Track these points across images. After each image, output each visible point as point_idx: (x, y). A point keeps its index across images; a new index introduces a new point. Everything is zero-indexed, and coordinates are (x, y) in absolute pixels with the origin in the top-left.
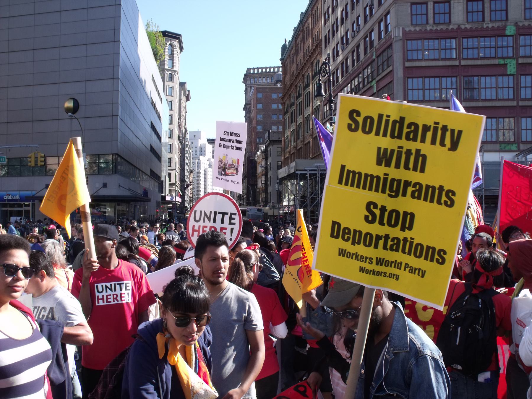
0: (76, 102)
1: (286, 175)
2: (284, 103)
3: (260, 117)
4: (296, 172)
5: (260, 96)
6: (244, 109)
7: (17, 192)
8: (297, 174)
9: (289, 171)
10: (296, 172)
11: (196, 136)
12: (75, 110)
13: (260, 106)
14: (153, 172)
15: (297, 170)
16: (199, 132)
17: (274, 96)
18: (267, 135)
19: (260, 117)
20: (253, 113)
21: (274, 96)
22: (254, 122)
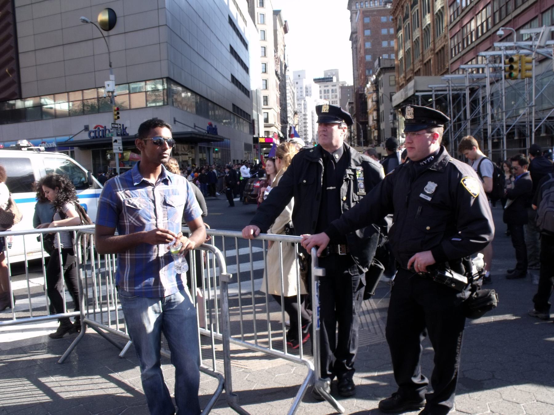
0: (111, 12)
1: (402, 100)
2: (396, 18)
3: (368, 45)
4: (417, 94)
5: (367, 20)
6: (351, 39)
7: (54, 139)
8: (418, 96)
9: (407, 94)
10: (417, 94)
11: (299, 76)
12: (110, 25)
13: (368, 33)
14: (238, 108)
15: (417, 91)
16: (303, 71)
17: (384, 19)
18: (377, 62)
19: (368, 45)
20: (361, 41)
21: (384, 19)
22: (362, 51)
